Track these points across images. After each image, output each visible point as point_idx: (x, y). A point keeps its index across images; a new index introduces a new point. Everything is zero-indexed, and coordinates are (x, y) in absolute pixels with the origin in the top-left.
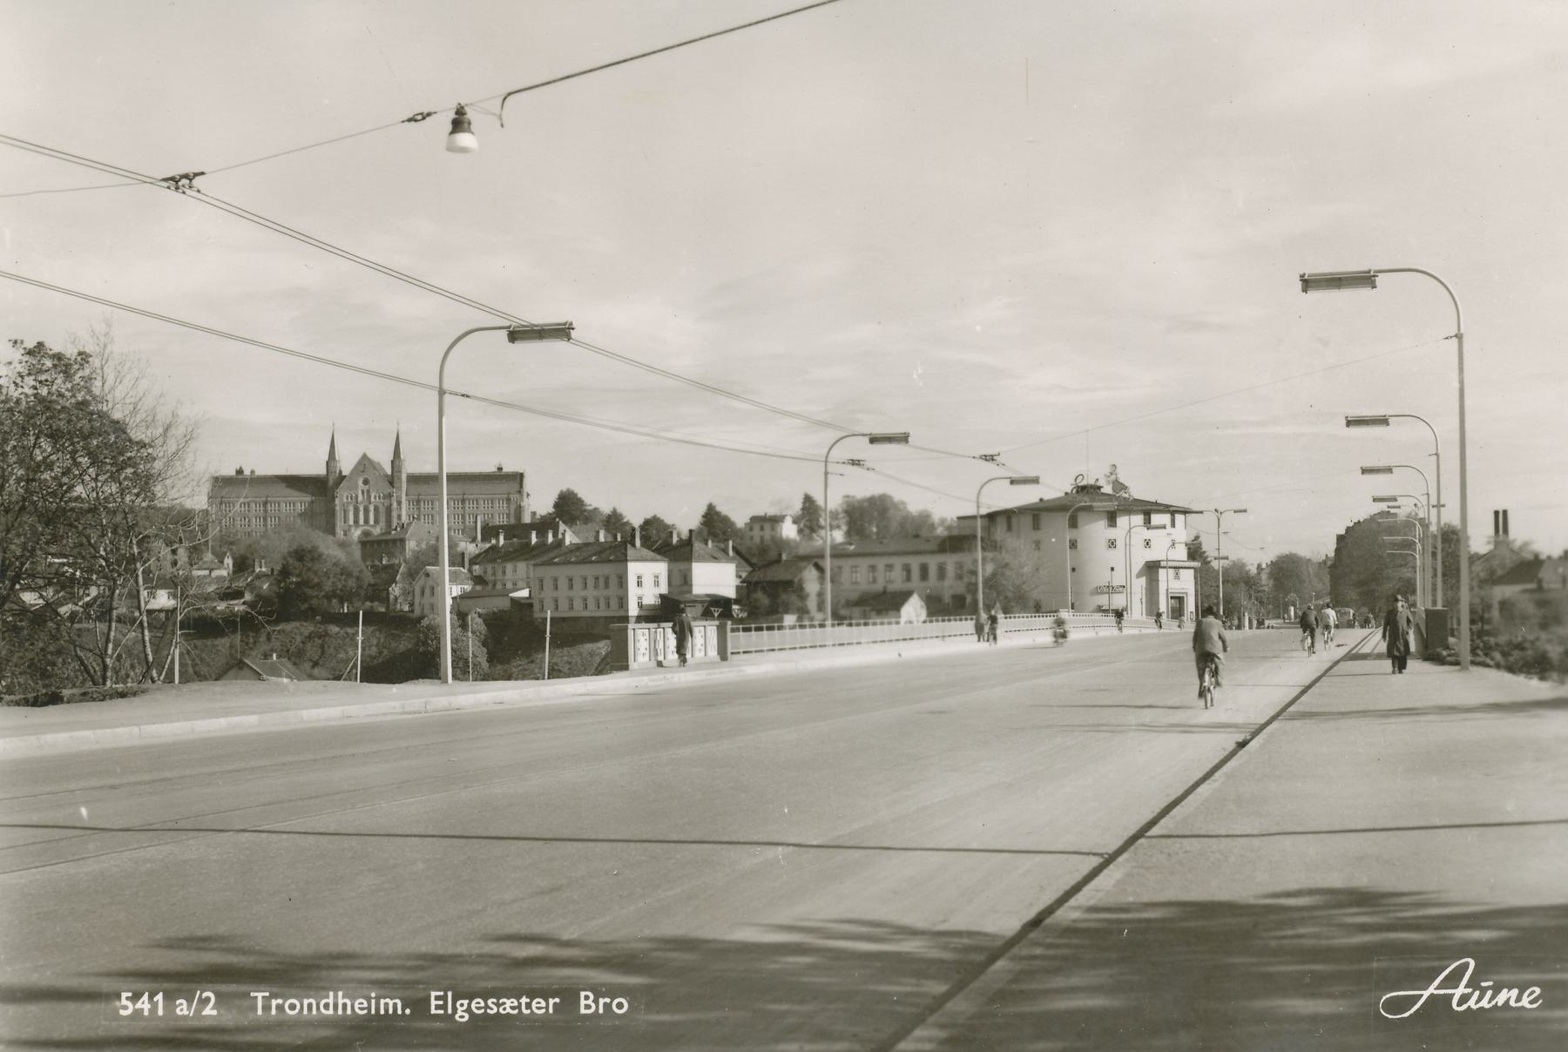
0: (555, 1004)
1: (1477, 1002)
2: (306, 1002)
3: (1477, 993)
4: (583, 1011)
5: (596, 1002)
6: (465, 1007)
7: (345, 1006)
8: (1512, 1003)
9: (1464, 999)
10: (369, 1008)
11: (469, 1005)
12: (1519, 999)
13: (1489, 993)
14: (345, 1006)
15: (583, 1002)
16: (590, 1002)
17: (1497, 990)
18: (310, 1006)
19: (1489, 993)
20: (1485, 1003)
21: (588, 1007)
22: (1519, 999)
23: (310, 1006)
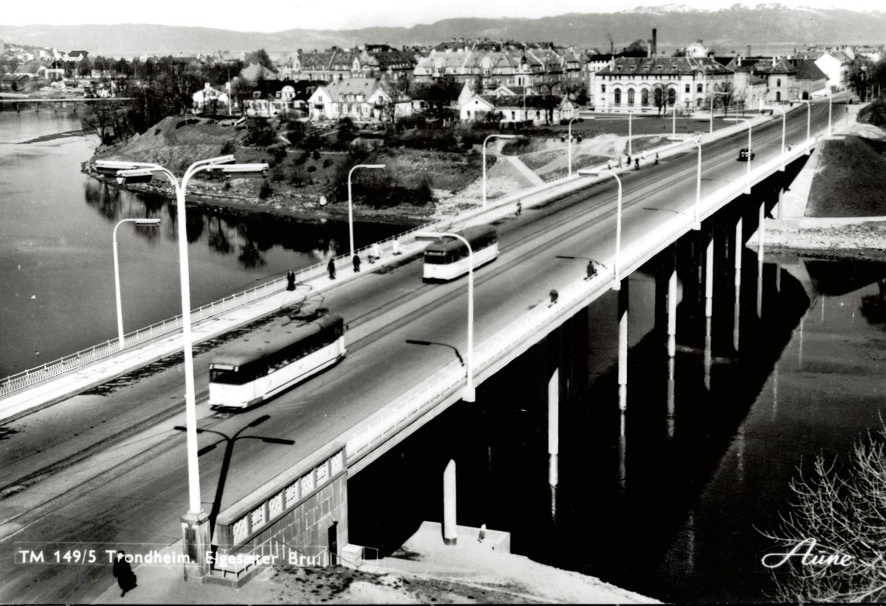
0: (275, 559)
1: (817, 561)
2: (137, 556)
3: (816, 557)
4: (291, 563)
5: (298, 558)
6: (225, 559)
7: (158, 559)
8: (835, 563)
9: (810, 558)
10: (172, 560)
11: (227, 559)
12: (839, 561)
13: (823, 557)
14: (158, 559)
15: (290, 558)
16: (295, 558)
17: (827, 556)
18: (139, 558)
19: (823, 557)
20: (820, 562)
21: (293, 560)
22: (839, 561)
23: (139, 558)
